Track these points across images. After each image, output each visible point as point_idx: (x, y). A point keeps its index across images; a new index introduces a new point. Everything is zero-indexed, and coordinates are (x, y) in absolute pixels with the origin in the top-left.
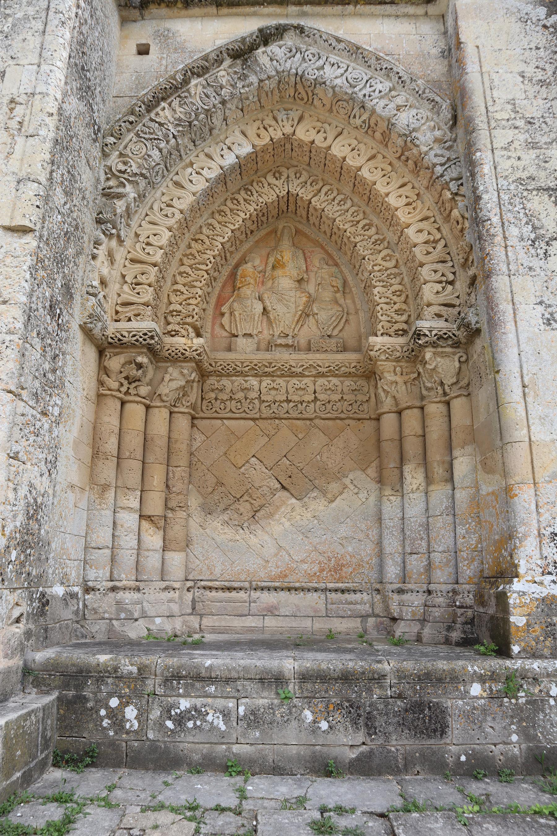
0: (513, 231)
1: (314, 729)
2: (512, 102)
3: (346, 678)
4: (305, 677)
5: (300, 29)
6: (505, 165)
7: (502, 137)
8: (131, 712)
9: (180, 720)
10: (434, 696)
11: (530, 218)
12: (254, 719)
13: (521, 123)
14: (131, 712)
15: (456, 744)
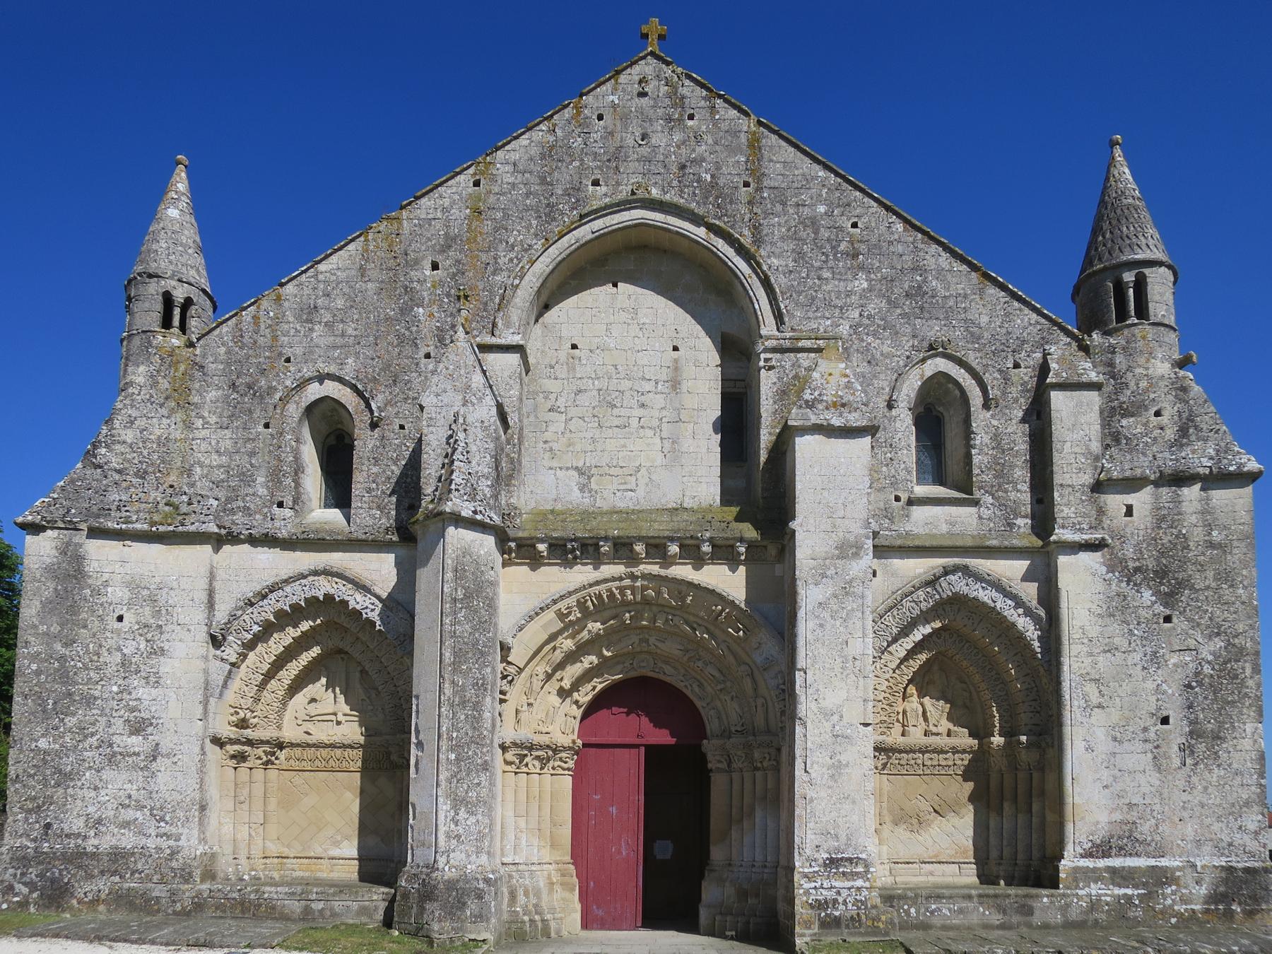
0: (1076, 703)
1: (984, 913)
2: (1082, 628)
3: (996, 896)
4: (980, 896)
5: (966, 571)
6: (1075, 666)
7: (1076, 649)
8: (913, 910)
9: (932, 913)
10: (1030, 902)
11: (1086, 697)
12: (961, 911)
13: (1086, 641)
14: (913, 910)
15: (1037, 919)
